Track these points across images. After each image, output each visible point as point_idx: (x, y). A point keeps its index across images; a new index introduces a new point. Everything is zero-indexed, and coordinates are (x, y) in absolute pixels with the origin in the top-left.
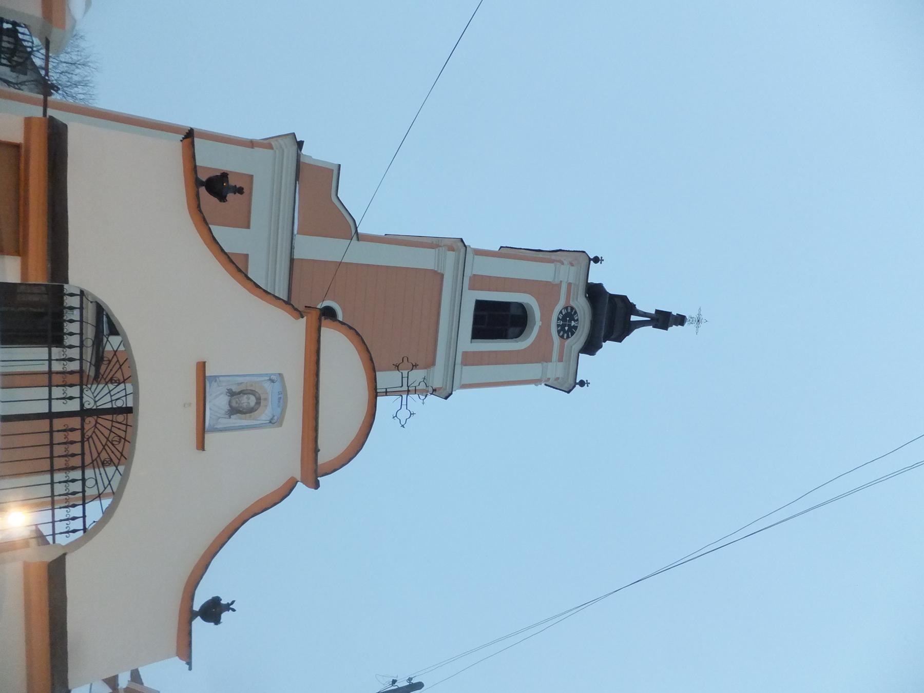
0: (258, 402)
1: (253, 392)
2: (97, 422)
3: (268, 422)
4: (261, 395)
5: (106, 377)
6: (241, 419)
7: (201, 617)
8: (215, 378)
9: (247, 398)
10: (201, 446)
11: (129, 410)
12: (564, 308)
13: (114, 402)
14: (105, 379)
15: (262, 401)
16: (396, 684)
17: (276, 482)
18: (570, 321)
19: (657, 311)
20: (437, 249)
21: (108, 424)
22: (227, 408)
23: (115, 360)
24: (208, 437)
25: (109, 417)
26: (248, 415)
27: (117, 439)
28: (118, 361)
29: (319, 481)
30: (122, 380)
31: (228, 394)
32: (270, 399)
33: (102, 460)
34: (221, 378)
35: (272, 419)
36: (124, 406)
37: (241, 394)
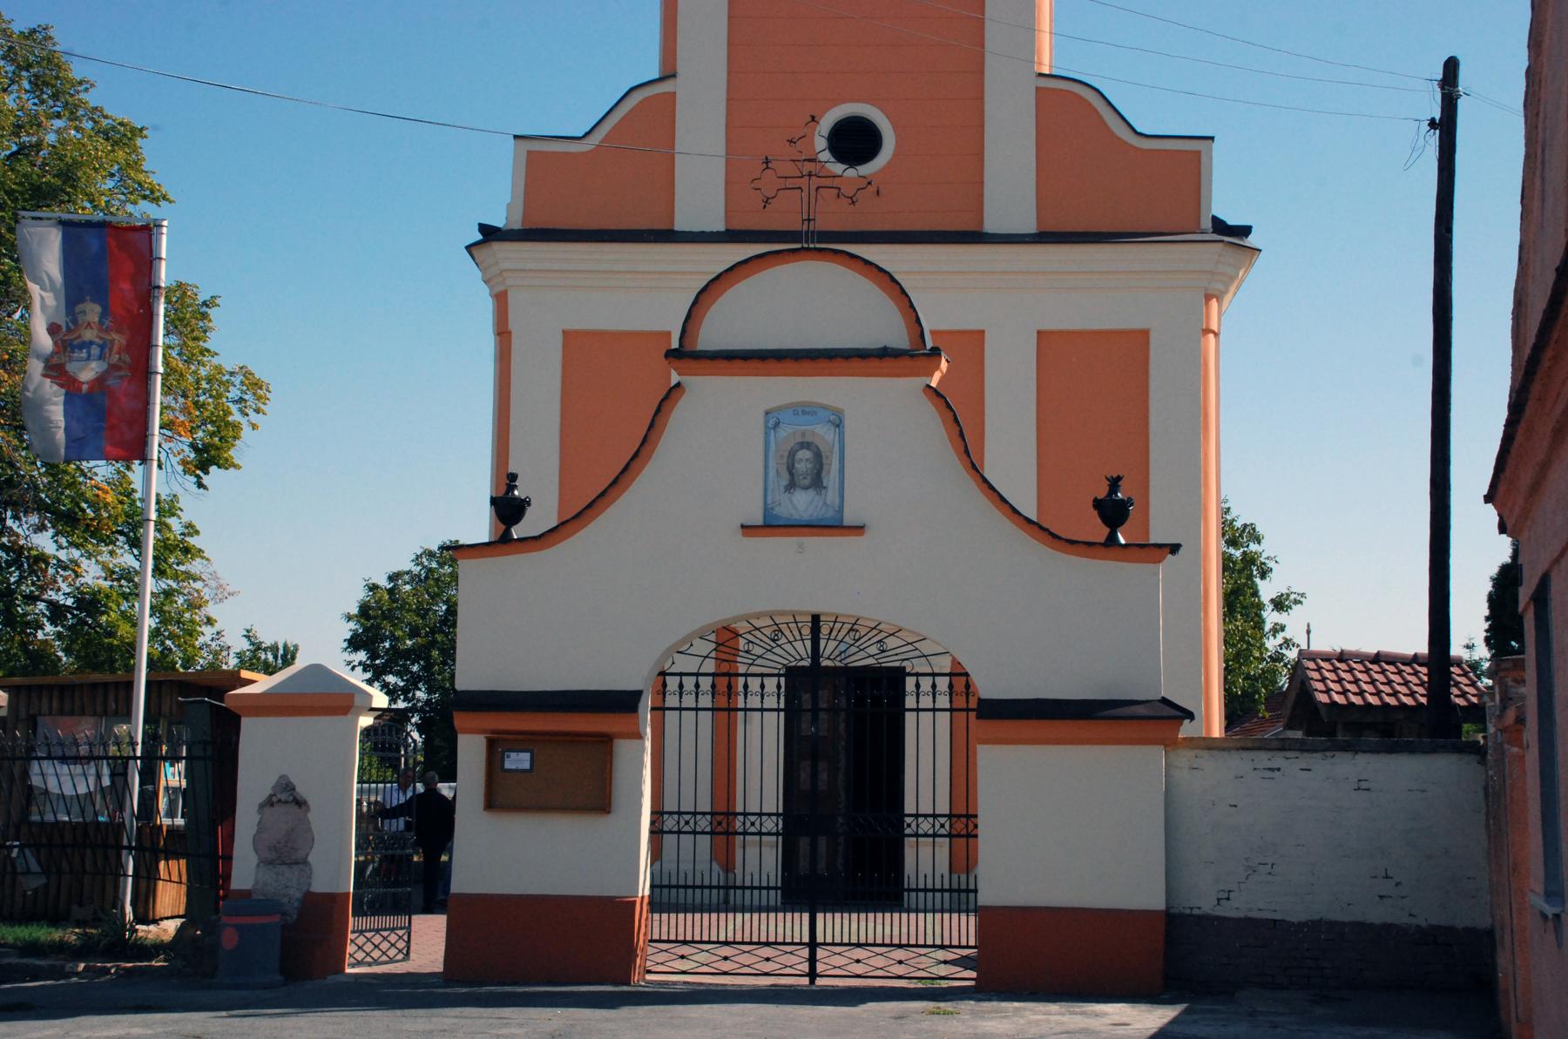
0: (805, 445)
1: (792, 454)
2: (828, 658)
3: (837, 429)
4: (796, 442)
6: (829, 472)
8: (767, 510)
9: (799, 463)
10: (859, 529)
11: (816, 619)
13: (804, 637)
14: (773, 648)
15: (805, 440)
21: (832, 644)
22: (811, 492)
23: (748, 636)
25: (822, 643)
27: (852, 634)
28: (749, 632)
30: (775, 628)
31: (792, 491)
32: (803, 428)
34: (769, 501)
35: (833, 424)
36: (810, 624)
37: (794, 471)
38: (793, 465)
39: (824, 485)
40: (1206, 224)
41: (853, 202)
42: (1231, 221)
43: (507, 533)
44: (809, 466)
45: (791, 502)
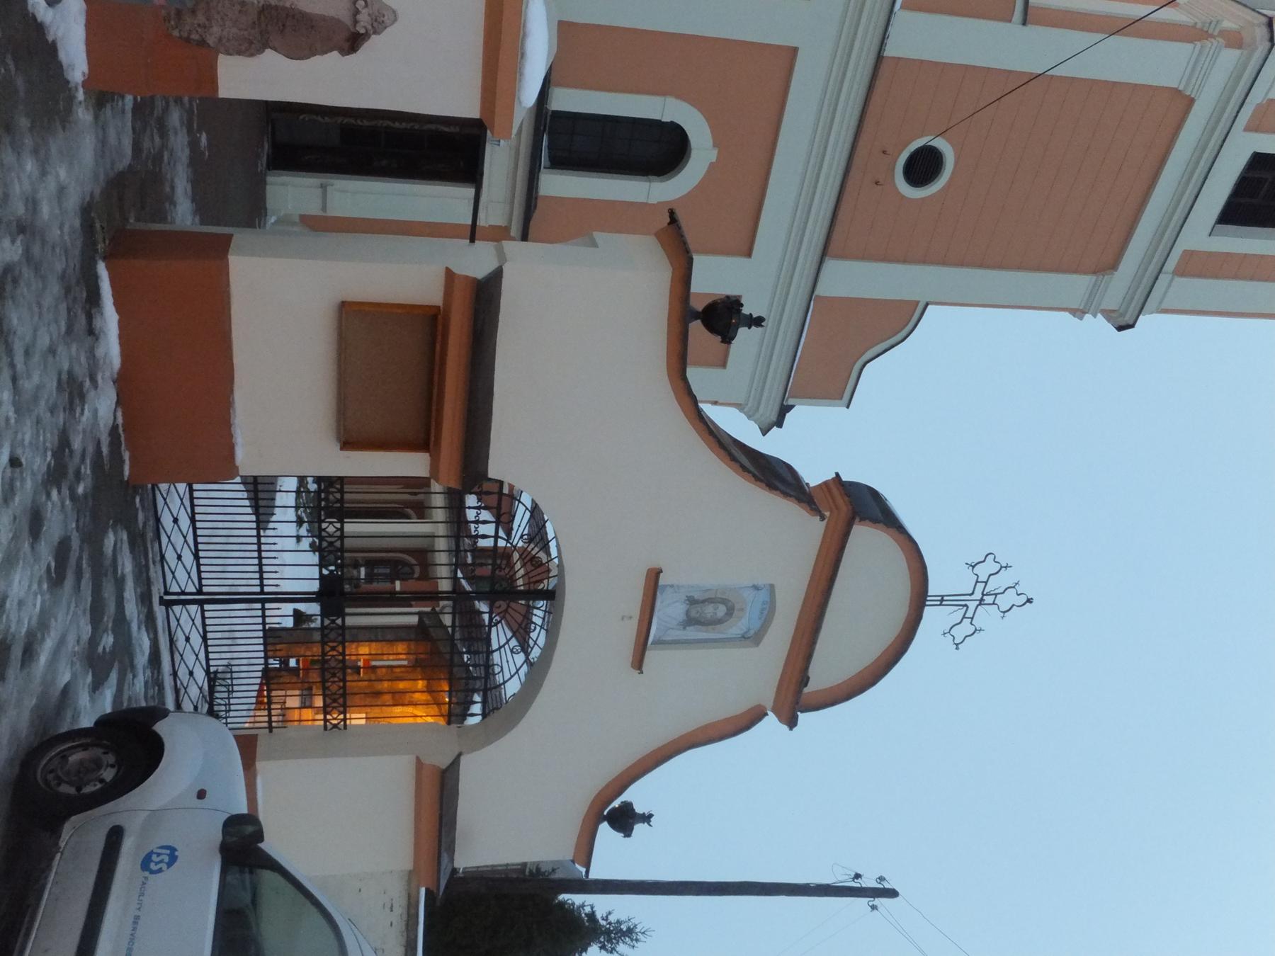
1: (724, 601)
2: (508, 606)
5: (525, 558)
7: (609, 823)
10: (638, 663)
15: (735, 612)
16: (859, 880)
17: (737, 706)
20: (1199, 44)
24: (650, 655)
26: (710, 627)
29: (798, 716)
31: (687, 602)
33: (511, 647)
35: (746, 632)
37: (707, 603)
38: (712, 602)
39: (688, 628)
40: (791, 402)
41: (945, 634)
42: (788, 415)
43: (696, 315)
44: (709, 616)
45: (677, 601)
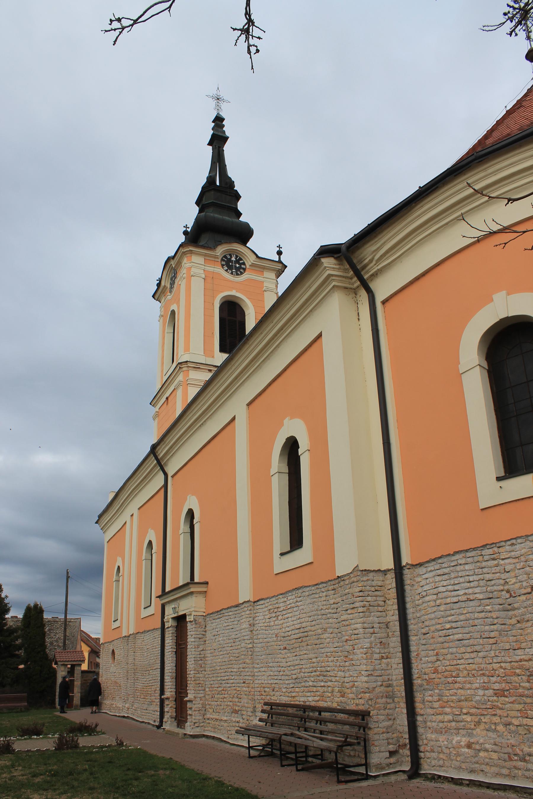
12: (223, 268)
18: (232, 262)
19: (209, 144)
